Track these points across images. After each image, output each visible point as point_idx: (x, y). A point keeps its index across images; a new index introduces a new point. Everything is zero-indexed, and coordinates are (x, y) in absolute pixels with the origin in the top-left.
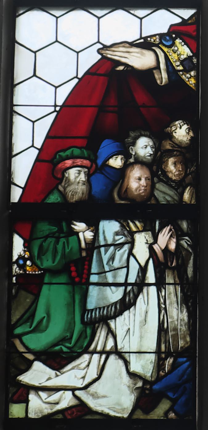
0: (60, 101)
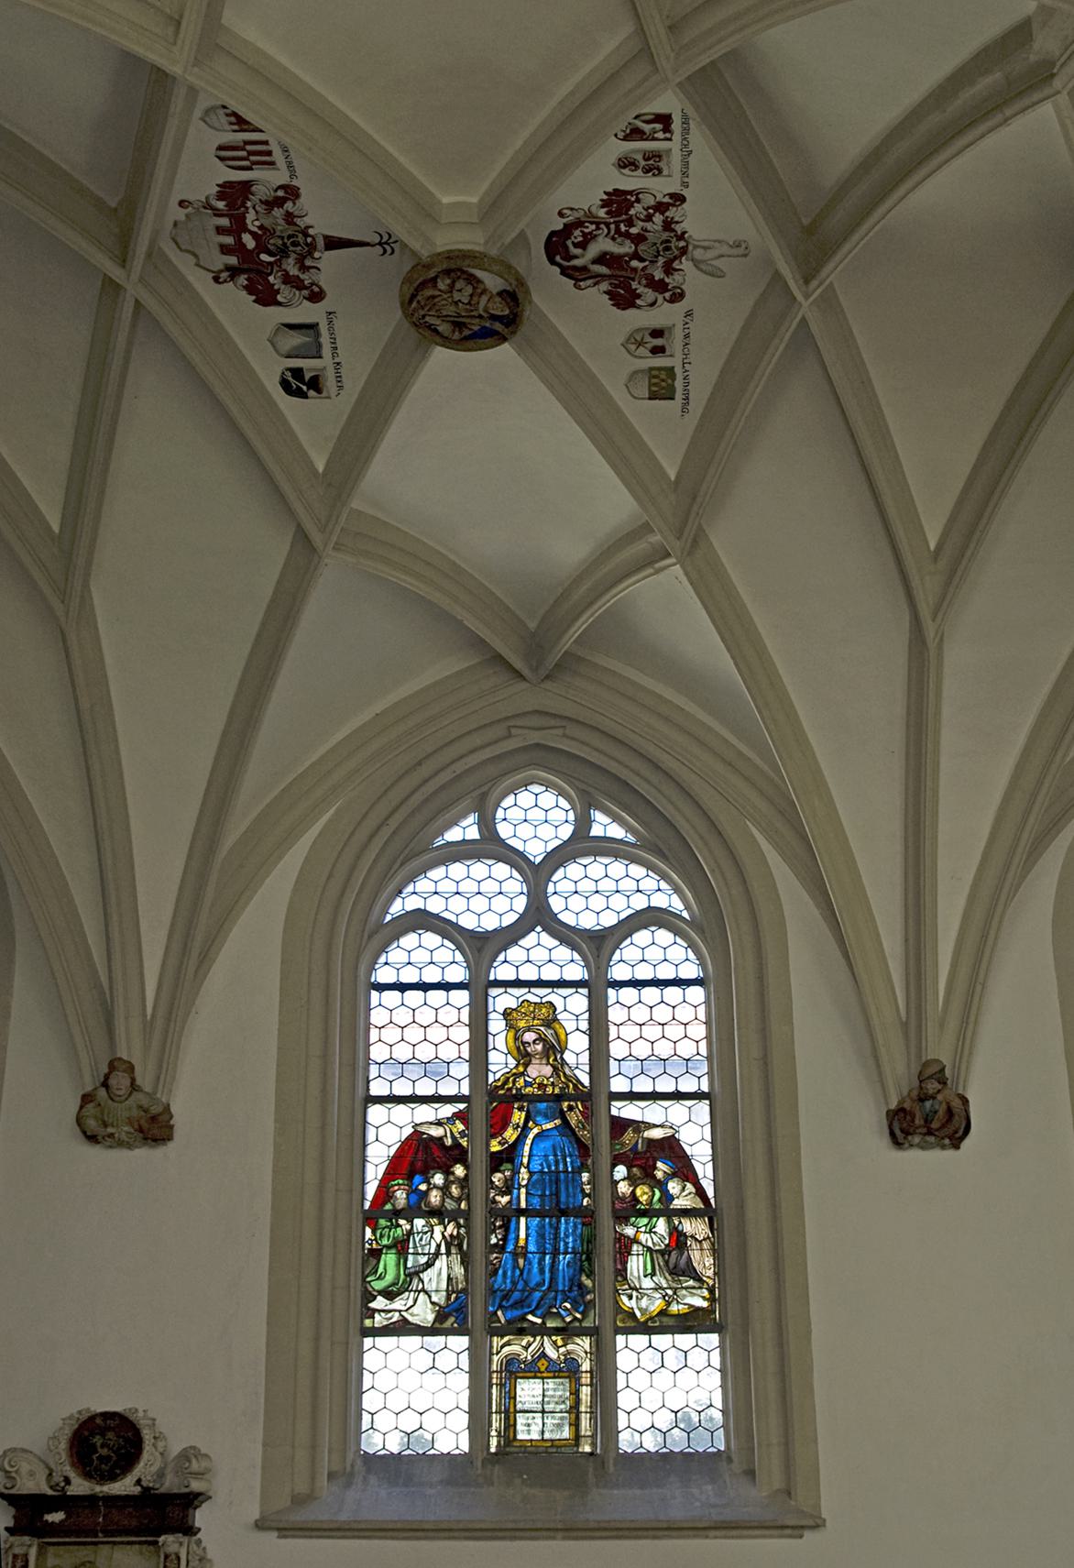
0: (391, 1155)
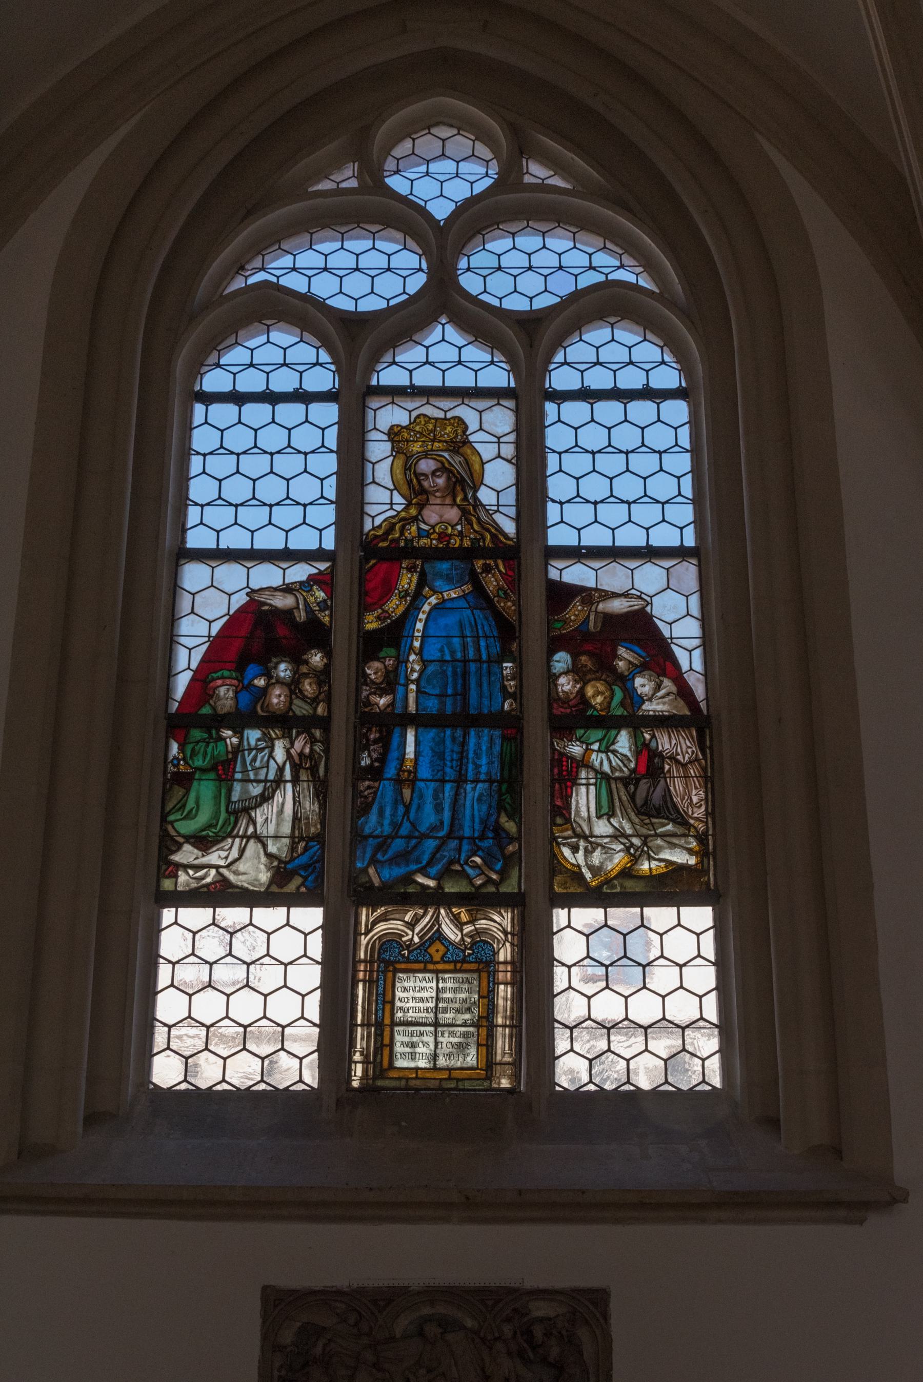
0: (214, 633)
